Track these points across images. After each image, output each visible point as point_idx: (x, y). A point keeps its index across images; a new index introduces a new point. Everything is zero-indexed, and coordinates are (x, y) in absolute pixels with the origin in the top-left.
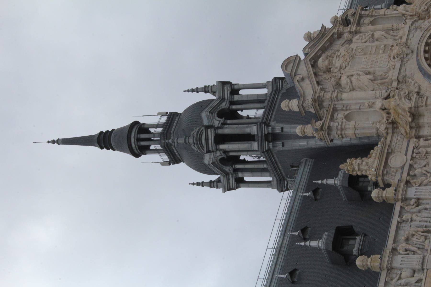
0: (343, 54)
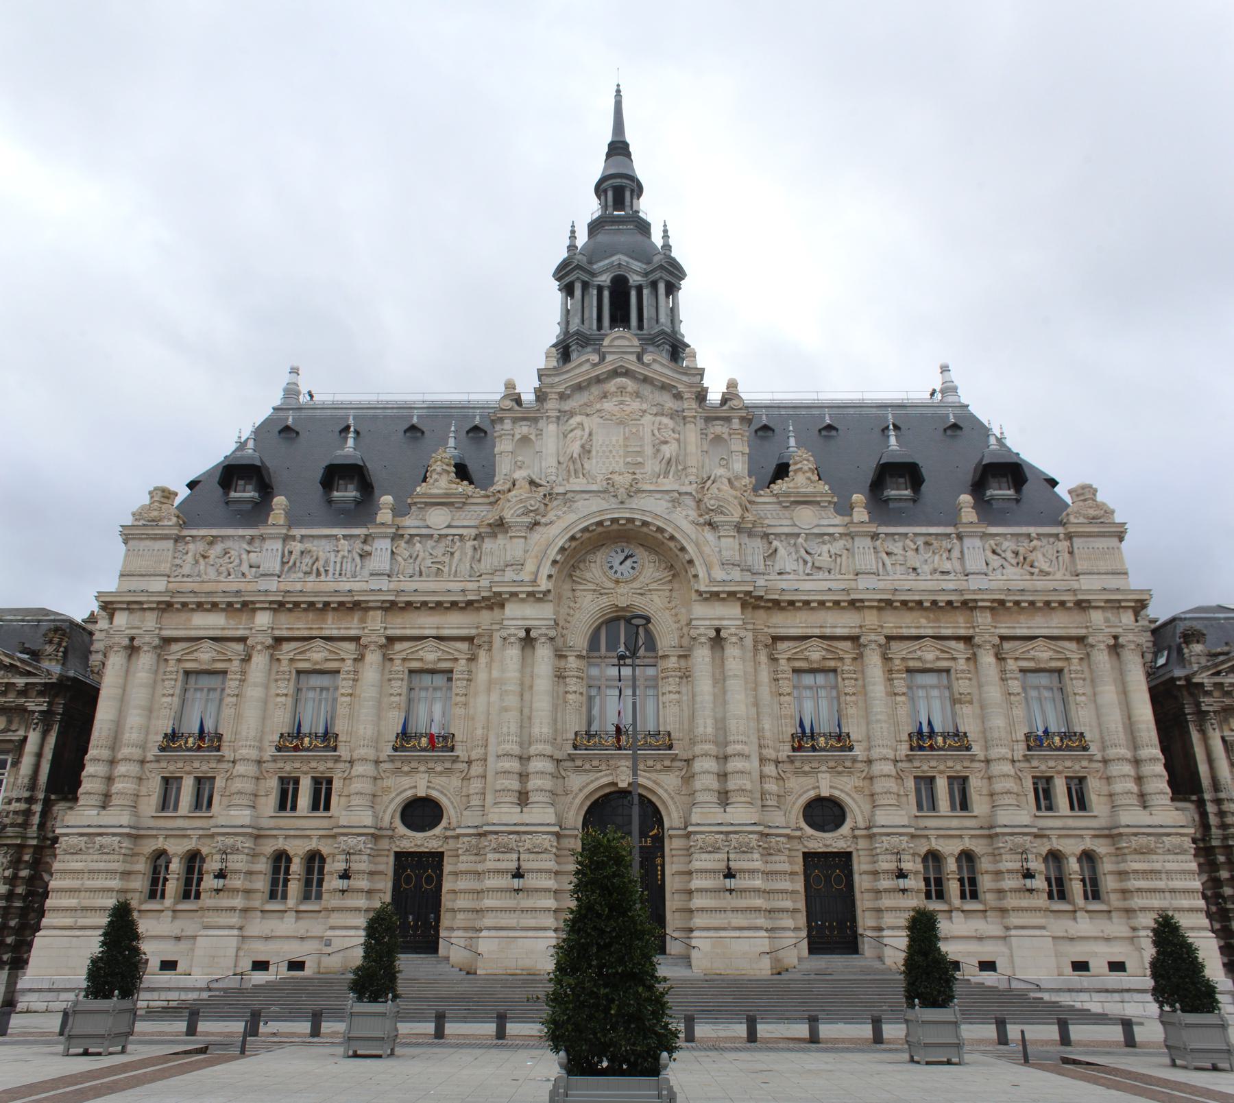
0: (625, 408)
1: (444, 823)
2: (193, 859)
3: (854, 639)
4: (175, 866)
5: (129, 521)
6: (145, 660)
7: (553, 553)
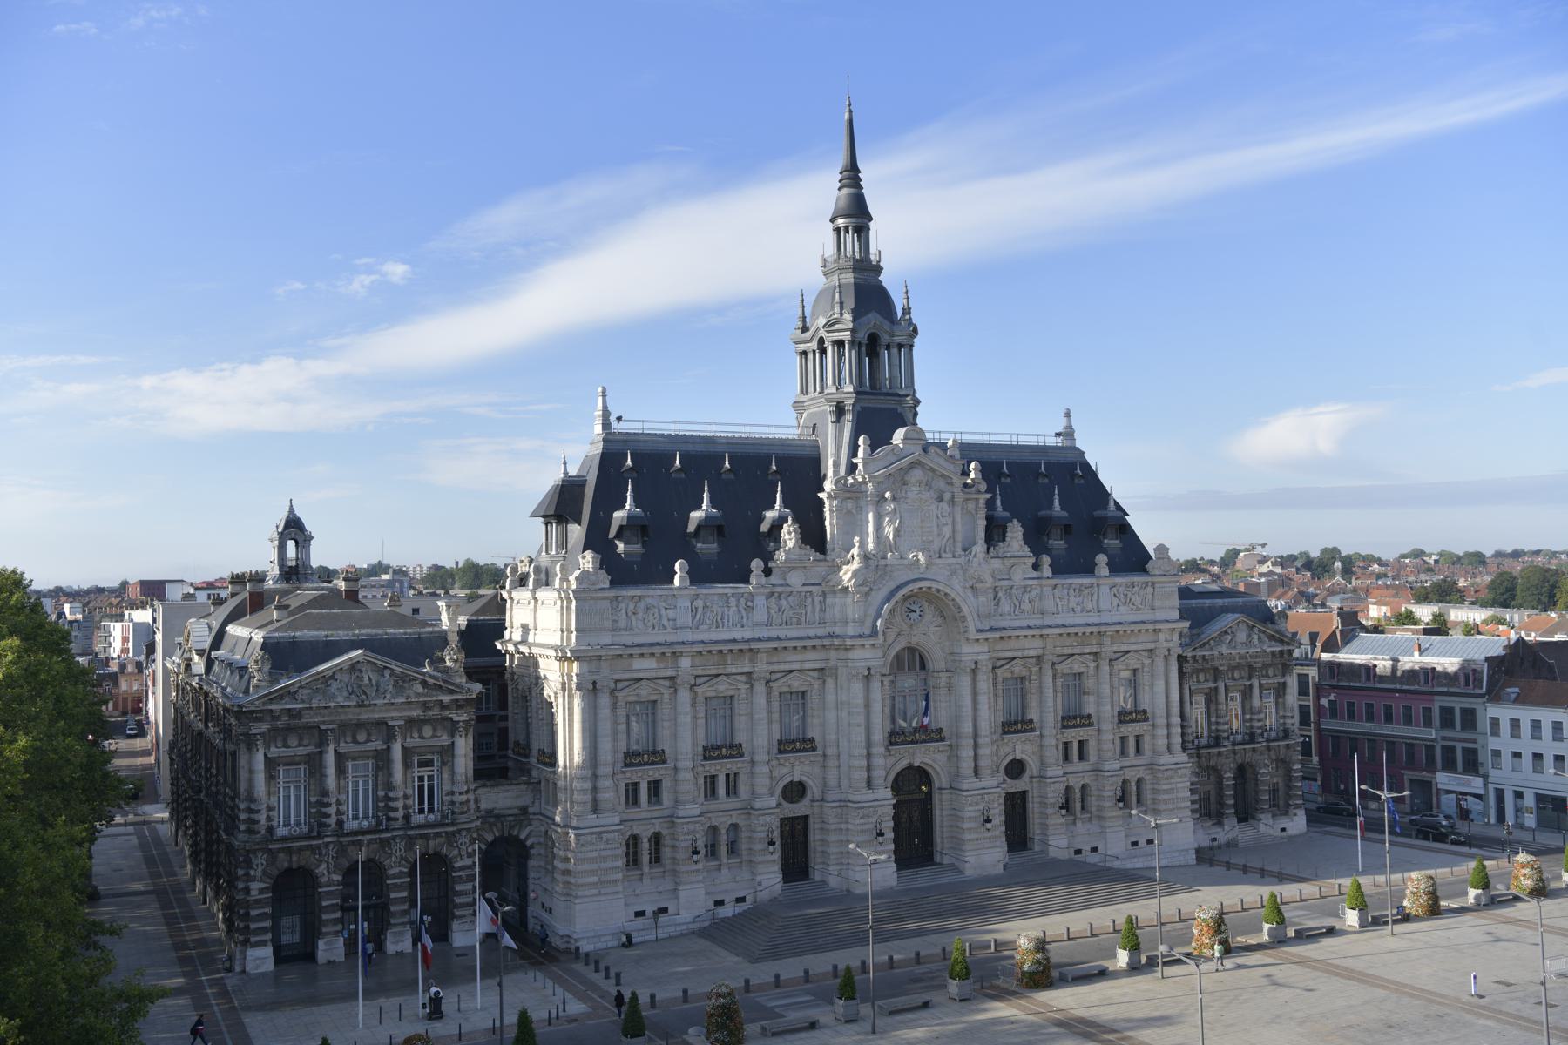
1: (809, 796)
2: (656, 839)
4: (645, 845)
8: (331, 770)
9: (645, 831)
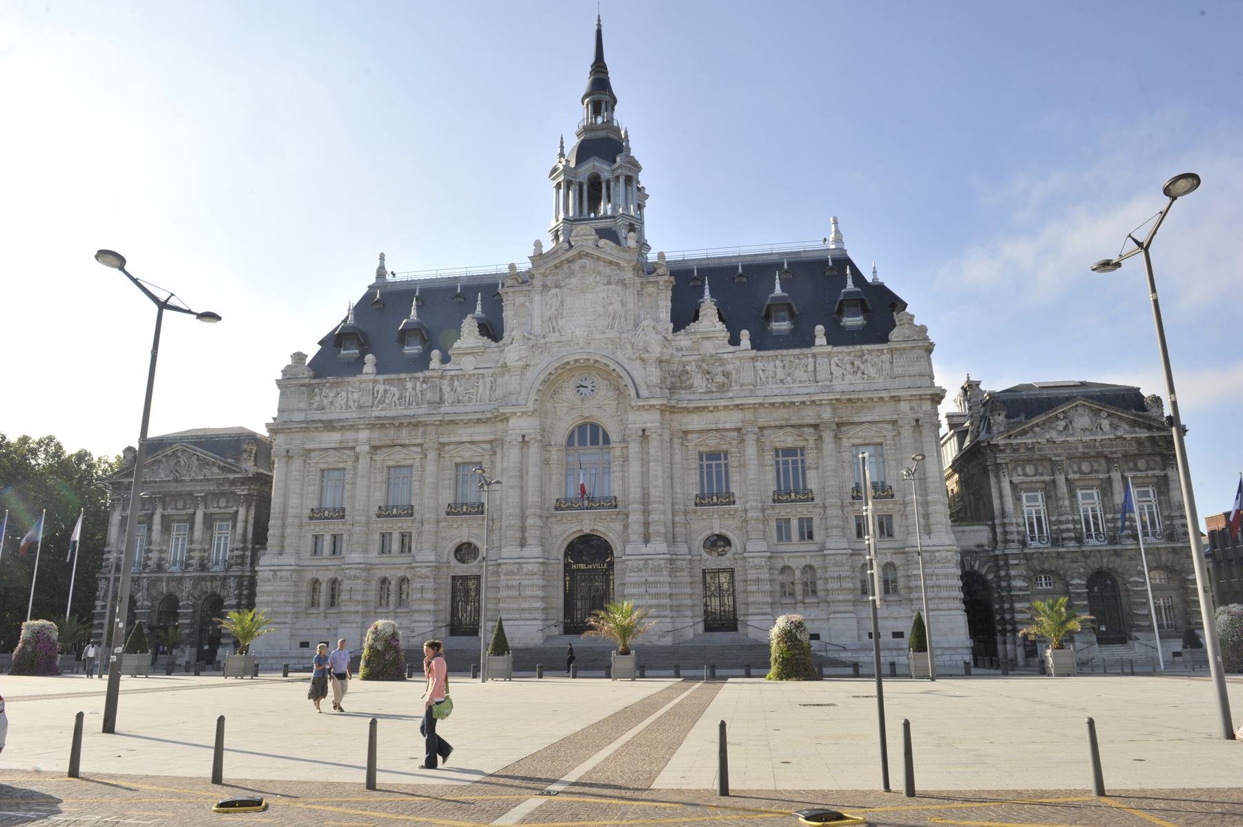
3: (738, 430)
5: (280, 377)
6: (297, 464)
7: (537, 385)
8: (157, 526)
9: (325, 577)
